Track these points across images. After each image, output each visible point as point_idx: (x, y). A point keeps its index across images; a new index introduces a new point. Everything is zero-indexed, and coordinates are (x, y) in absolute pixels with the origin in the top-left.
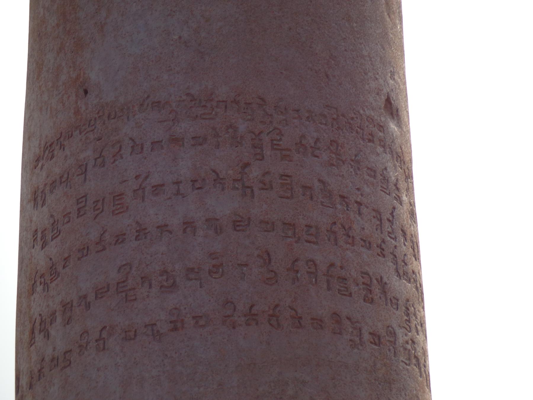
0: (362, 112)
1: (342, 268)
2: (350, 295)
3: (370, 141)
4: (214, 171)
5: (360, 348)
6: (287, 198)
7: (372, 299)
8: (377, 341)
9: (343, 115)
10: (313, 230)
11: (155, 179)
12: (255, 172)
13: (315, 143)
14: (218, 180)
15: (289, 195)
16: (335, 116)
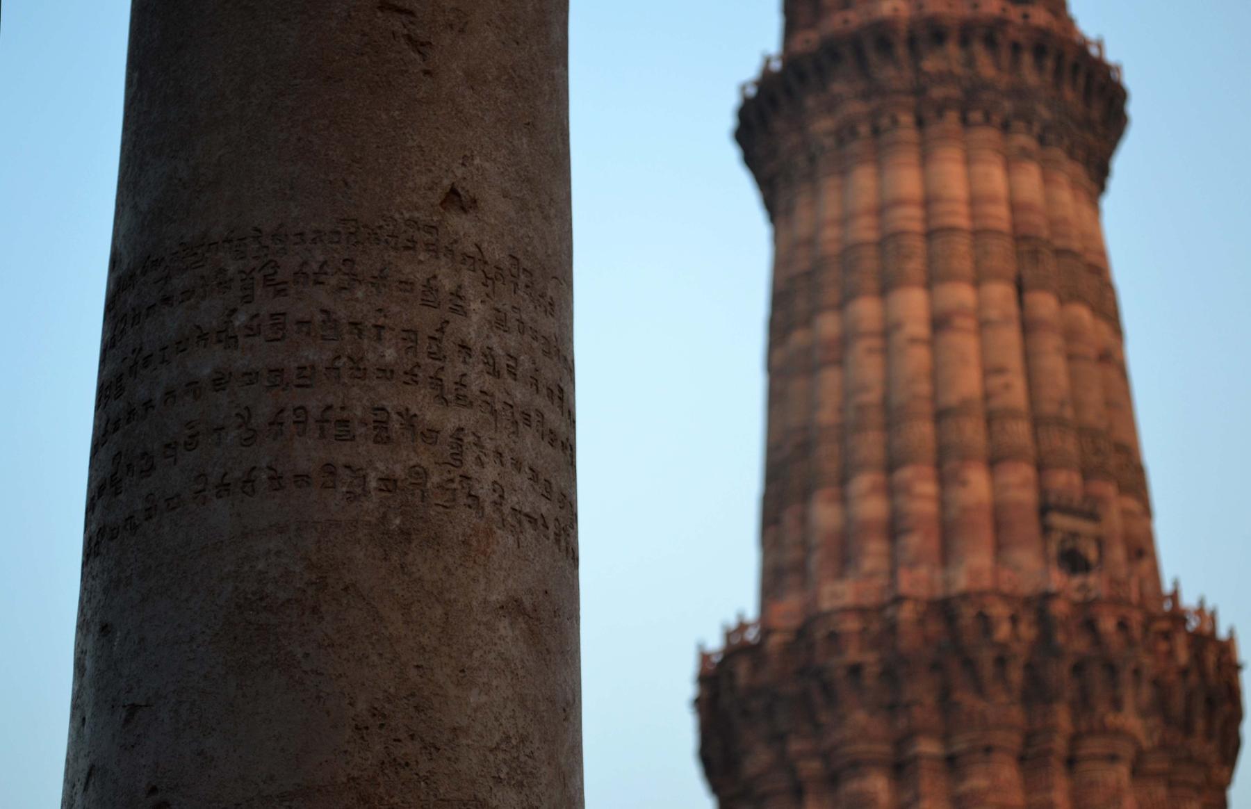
0: (397, 216)
1: (343, 408)
2: (353, 438)
3: (407, 248)
4: (198, 327)
5: (363, 499)
6: (278, 340)
7: (388, 437)
8: (391, 487)
9: (365, 226)
10: (307, 372)
11: (145, 353)
12: (241, 319)
13: (321, 267)
14: (203, 337)
15: (279, 336)
16: (352, 230)
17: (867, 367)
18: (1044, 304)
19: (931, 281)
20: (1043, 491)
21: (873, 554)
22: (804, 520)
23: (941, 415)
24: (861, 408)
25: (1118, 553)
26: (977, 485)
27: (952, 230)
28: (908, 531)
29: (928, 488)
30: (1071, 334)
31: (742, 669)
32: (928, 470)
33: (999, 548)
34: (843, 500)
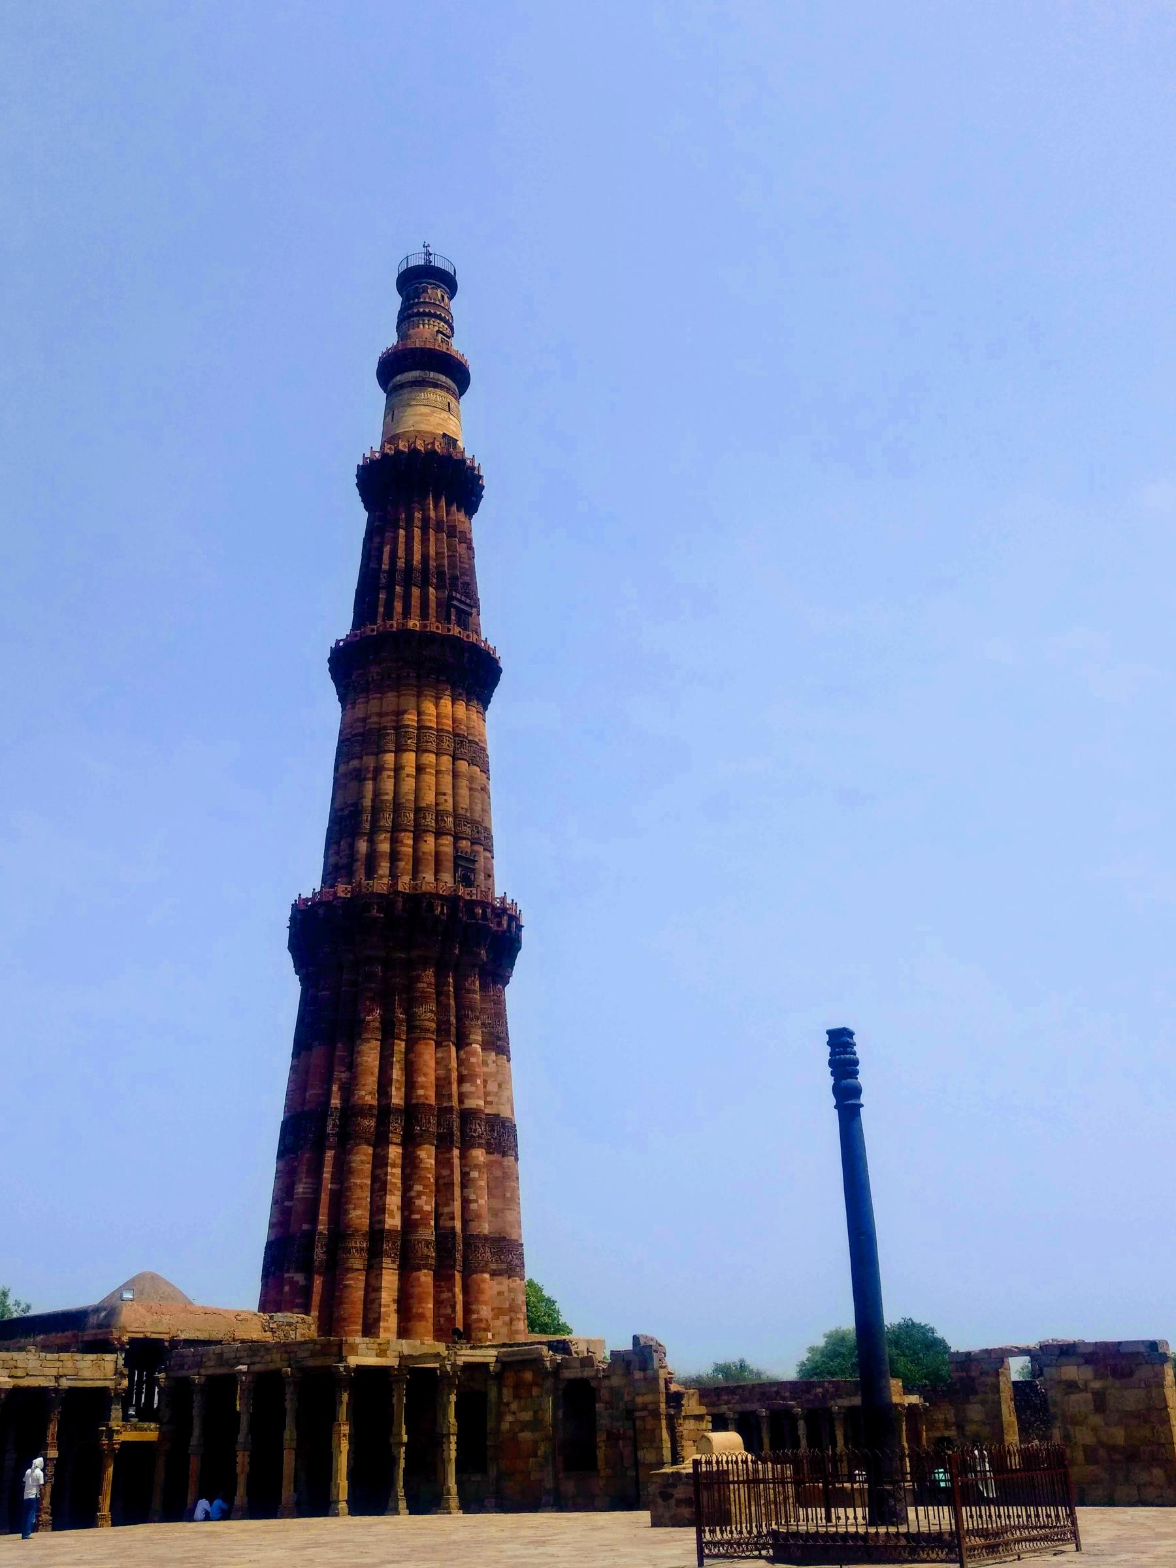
17: (389, 785)
18: (463, 766)
19: (420, 750)
20: (456, 848)
21: (384, 867)
22: (352, 846)
23: (418, 810)
24: (382, 801)
25: (482, 876)
26: (429, 844)
27: (431, 728)
28: (399, 860)
29: (411, 842)
30: (472, 779)
31: (321, 911)
32: (411, 835)
33: (437, 872)
34: (372, 842)
